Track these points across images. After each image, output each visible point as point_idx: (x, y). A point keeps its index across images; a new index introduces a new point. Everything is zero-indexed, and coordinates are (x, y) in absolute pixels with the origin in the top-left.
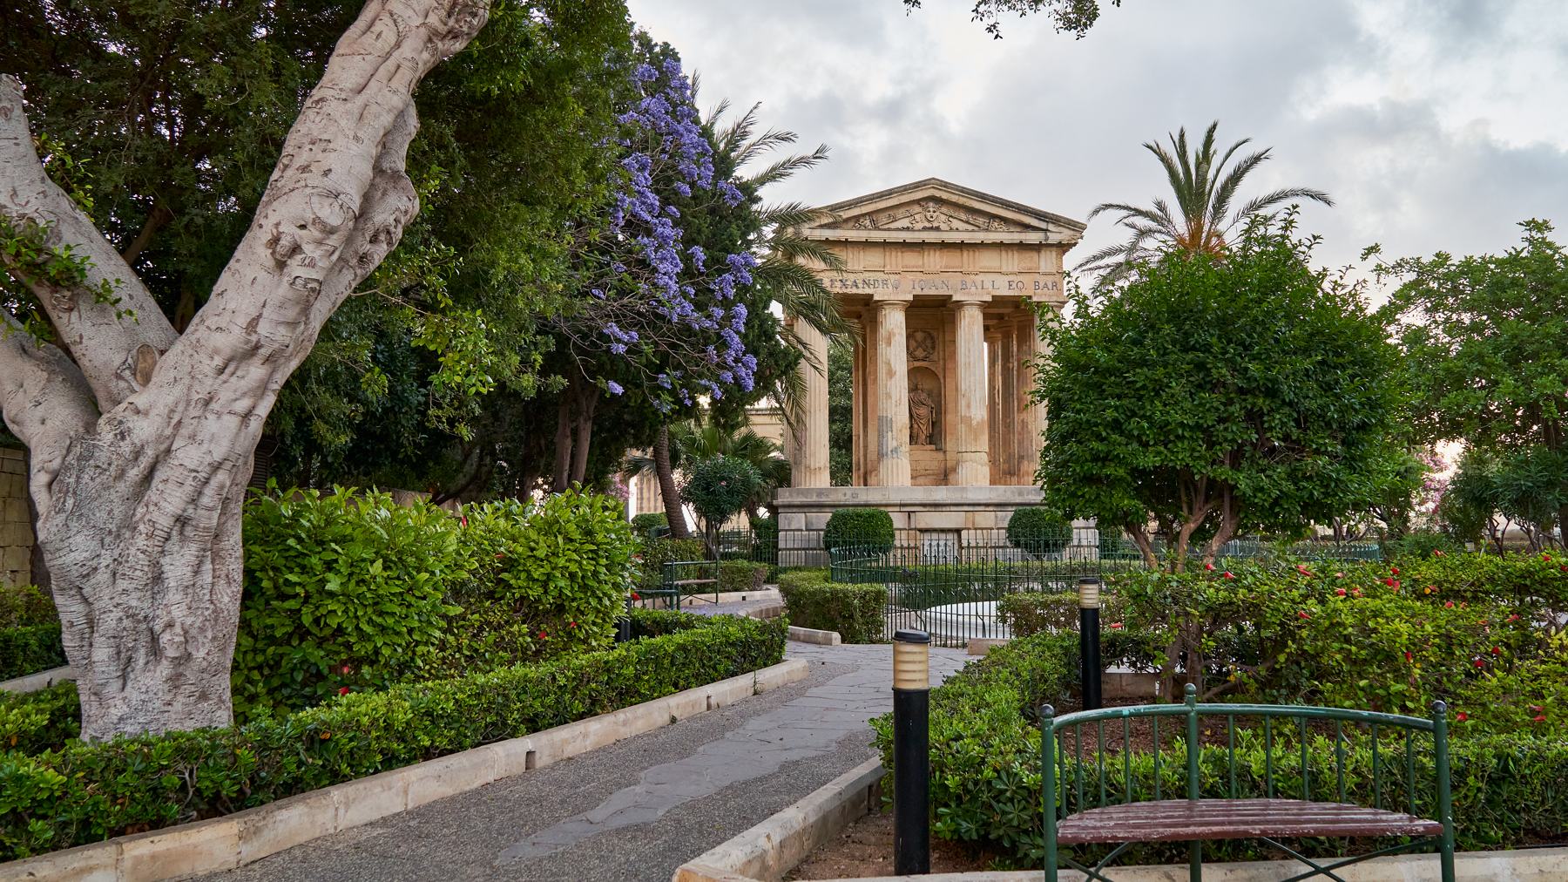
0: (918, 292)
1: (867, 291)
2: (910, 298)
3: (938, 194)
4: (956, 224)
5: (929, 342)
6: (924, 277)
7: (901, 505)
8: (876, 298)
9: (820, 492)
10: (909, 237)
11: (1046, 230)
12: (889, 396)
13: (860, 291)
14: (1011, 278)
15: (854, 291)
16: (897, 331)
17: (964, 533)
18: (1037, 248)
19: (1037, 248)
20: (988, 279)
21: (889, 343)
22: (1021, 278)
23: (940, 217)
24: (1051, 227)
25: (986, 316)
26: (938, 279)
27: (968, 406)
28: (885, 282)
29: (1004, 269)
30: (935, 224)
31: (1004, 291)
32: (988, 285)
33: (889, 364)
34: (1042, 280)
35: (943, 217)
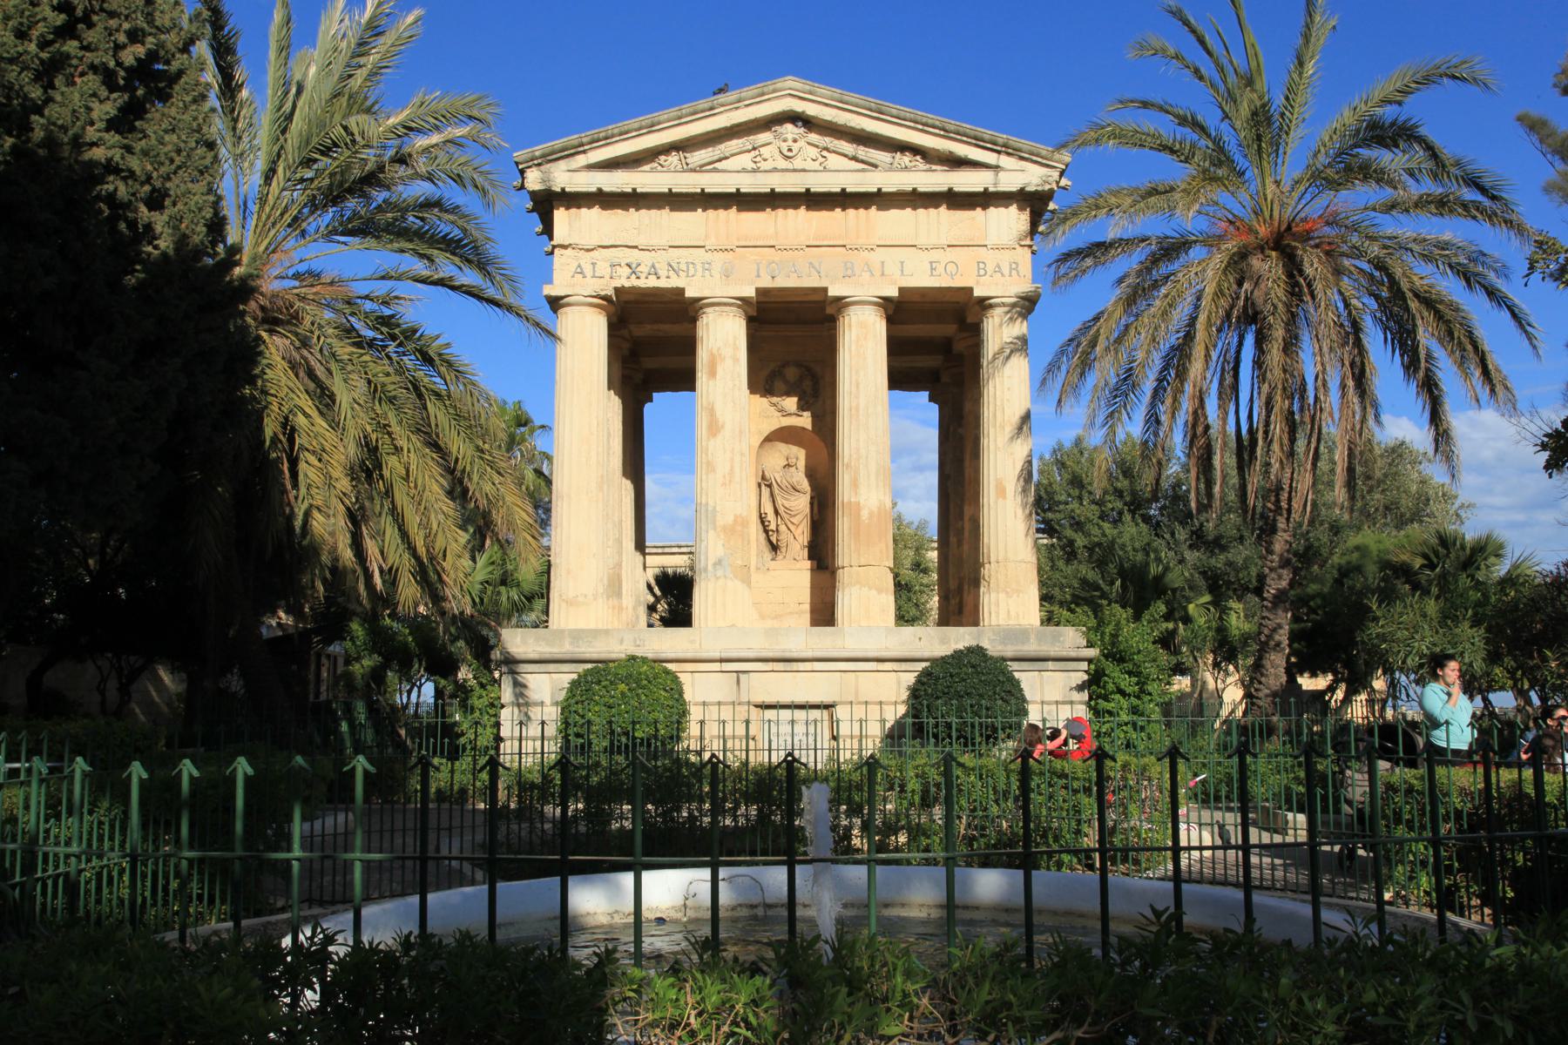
0: (766, 283)
3: (799, 106)
4: (834, 161)
5: (807, 384)
7: (722, 661)
8: (689, 294)
9: (577, 635)
10: (749, 184)
11: (996, 168)
12: (711, 467)
13: (663, 283)
14: (935, 255)
15: (652, 283)
17: (841, 712)
18: (985, 199)
19: (985, 199)
20: (891, 257)
21: (713, 373)
22: (952, 254)
23: (806, 146)
24: (1005, 161)
25: (891, 321)
27: (855, 484)
28: (707, 266)
29: (922, 241)
30: (798, 163)
31: (921, 278)
32: (892, 269)
33: (712, 412)
34: (991, 258)
35: (813, 152)
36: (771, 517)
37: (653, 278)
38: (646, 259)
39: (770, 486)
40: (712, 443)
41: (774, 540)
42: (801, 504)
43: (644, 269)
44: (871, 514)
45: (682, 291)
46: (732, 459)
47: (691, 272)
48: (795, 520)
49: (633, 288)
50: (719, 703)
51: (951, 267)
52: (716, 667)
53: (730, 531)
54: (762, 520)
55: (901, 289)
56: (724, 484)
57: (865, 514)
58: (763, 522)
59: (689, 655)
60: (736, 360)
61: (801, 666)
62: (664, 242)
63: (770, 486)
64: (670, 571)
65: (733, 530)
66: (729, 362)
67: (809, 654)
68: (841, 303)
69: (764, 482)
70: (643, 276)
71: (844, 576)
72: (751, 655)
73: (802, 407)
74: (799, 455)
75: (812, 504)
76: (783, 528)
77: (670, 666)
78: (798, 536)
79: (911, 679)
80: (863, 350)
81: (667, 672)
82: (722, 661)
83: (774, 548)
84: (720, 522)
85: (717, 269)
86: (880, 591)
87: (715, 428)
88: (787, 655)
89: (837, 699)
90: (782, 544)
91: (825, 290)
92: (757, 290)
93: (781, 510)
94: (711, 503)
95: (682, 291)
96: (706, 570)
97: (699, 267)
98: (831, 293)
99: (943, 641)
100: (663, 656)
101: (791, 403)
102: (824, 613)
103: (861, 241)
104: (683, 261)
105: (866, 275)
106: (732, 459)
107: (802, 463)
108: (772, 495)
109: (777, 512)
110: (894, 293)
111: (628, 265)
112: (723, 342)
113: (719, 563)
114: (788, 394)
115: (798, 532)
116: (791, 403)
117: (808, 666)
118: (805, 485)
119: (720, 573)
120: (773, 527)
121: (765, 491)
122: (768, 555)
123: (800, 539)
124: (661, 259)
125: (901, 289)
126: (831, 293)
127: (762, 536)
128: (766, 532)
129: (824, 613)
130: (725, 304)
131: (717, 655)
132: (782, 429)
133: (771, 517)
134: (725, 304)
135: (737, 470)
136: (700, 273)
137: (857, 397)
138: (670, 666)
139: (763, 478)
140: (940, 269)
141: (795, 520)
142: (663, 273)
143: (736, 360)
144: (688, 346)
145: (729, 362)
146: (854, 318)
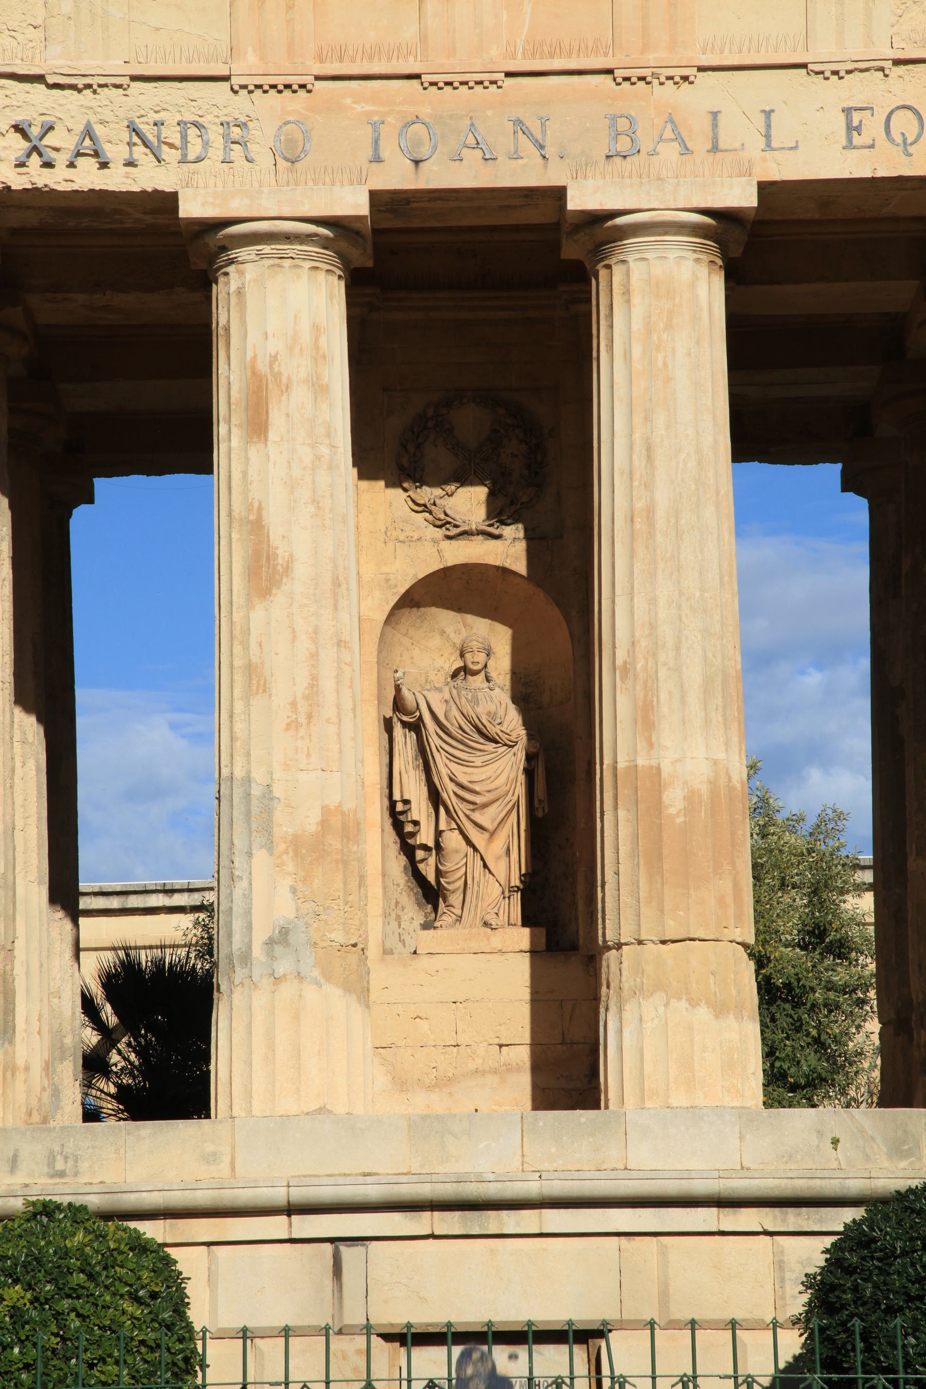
0: (397, 177)
1: (148, 177)
2: (354, 203)
6: (428, 103)
7: (291, 1210)
8: (191, 208)
12: (257, 680)
13: (116, 180)
14: (858, 89)
15: (87, 178)
16: (296, 368)
21: (258, 427)
25: (737, 275)
26: (491, 110)
27: (646, 720)
28: (236, 134)
29: (822, 50)
31: (821, 155)
32: (741, 132)
33: (257, 527)
36: (420, 809)
37: (87, 165)
38: (70, 110)
39: (416, 727)
40: (258, 615)
41: (428, 871)
42: (500, 775)
43: (62, 140)
44: (691, 799)
45: (170, 200)
46: (314, 655)
47: (195, 149)
49: (35, 192)
50: (287, 1332)
51: (904, 123)
52: (276, 1226)
53: (309, 851)
54: (397, 817)
55: (764, 188)
56: (292, 726)
57: (674, 799)
58: (398, 826)
59: (202, 1198)
60: (320, 389)
61: (511, 1221)
62: (115, 66)
63: (416, 727)
64: (144, 958)
65: (319, 849)
66: (300, 396)
67: (532, 1188)
68: (601, 232)
70: (61, 160)
71: (621, 969)
72: (373, 1192)
73: (501, 511)
74: (495, 641)
75: (529, 773)
76: (452, 840)
77: (151, 1230)
78: (493, 858)
79: (811, 1255)
80: (662, 355)
81: (142, 1247)
82: (291, 1210)
83: (431, 894)
84: (284, 826)
85: (262, 141)
86: (720, 1010)
87: (266, 574)
88: (472, 1190)
89: (608, 1313)
90: (452, 883)
91: (559, 193)
92: (375, 196)
93: (448, 791)
94: (259, 776)
95: (172, 198)
96: (246, 958)
97: (215, 135)
98: (576, 202)
99: (901, 1147)
100: (130, 1201)
101: (469, 502)
102: (568, 1073)
103: (652, 58)
104: (170, 118)
105: (669, 152)
106: (314, 655)
107: (501, 664)
108: (422, 751)
109: (435, 798)
110: (743, 197)
111: (17, 128)
112: (285, 334)
113: (281, 938)
114: (463, 479)
115: (494, 850)
116: (469, 502)
117: (527, 1220)
118: (512, 722)
119: (283, 966)
120: (426, 836)
121: (405, 742)
122: (413, 913)
123: (499, 868)
124: (110, 113)
125: (764, 188)
126: (576, 202)
127: (397, 863)
128: (408, 850)
129: (568, 1073)
130: (288, 238)
131: (278, 1195)
132: (446, 573)
133: (420, 809)
134: (288, 238)
135: (328, 684)
136: (216, 152)
137: (649, 486)
138: (151, 1230)
139: (398, 704)
140: (873, 127)
142: (115, 152)
143: (320, 389)
144: (190, 350)
145: (300, 396)
146: (637, 269)
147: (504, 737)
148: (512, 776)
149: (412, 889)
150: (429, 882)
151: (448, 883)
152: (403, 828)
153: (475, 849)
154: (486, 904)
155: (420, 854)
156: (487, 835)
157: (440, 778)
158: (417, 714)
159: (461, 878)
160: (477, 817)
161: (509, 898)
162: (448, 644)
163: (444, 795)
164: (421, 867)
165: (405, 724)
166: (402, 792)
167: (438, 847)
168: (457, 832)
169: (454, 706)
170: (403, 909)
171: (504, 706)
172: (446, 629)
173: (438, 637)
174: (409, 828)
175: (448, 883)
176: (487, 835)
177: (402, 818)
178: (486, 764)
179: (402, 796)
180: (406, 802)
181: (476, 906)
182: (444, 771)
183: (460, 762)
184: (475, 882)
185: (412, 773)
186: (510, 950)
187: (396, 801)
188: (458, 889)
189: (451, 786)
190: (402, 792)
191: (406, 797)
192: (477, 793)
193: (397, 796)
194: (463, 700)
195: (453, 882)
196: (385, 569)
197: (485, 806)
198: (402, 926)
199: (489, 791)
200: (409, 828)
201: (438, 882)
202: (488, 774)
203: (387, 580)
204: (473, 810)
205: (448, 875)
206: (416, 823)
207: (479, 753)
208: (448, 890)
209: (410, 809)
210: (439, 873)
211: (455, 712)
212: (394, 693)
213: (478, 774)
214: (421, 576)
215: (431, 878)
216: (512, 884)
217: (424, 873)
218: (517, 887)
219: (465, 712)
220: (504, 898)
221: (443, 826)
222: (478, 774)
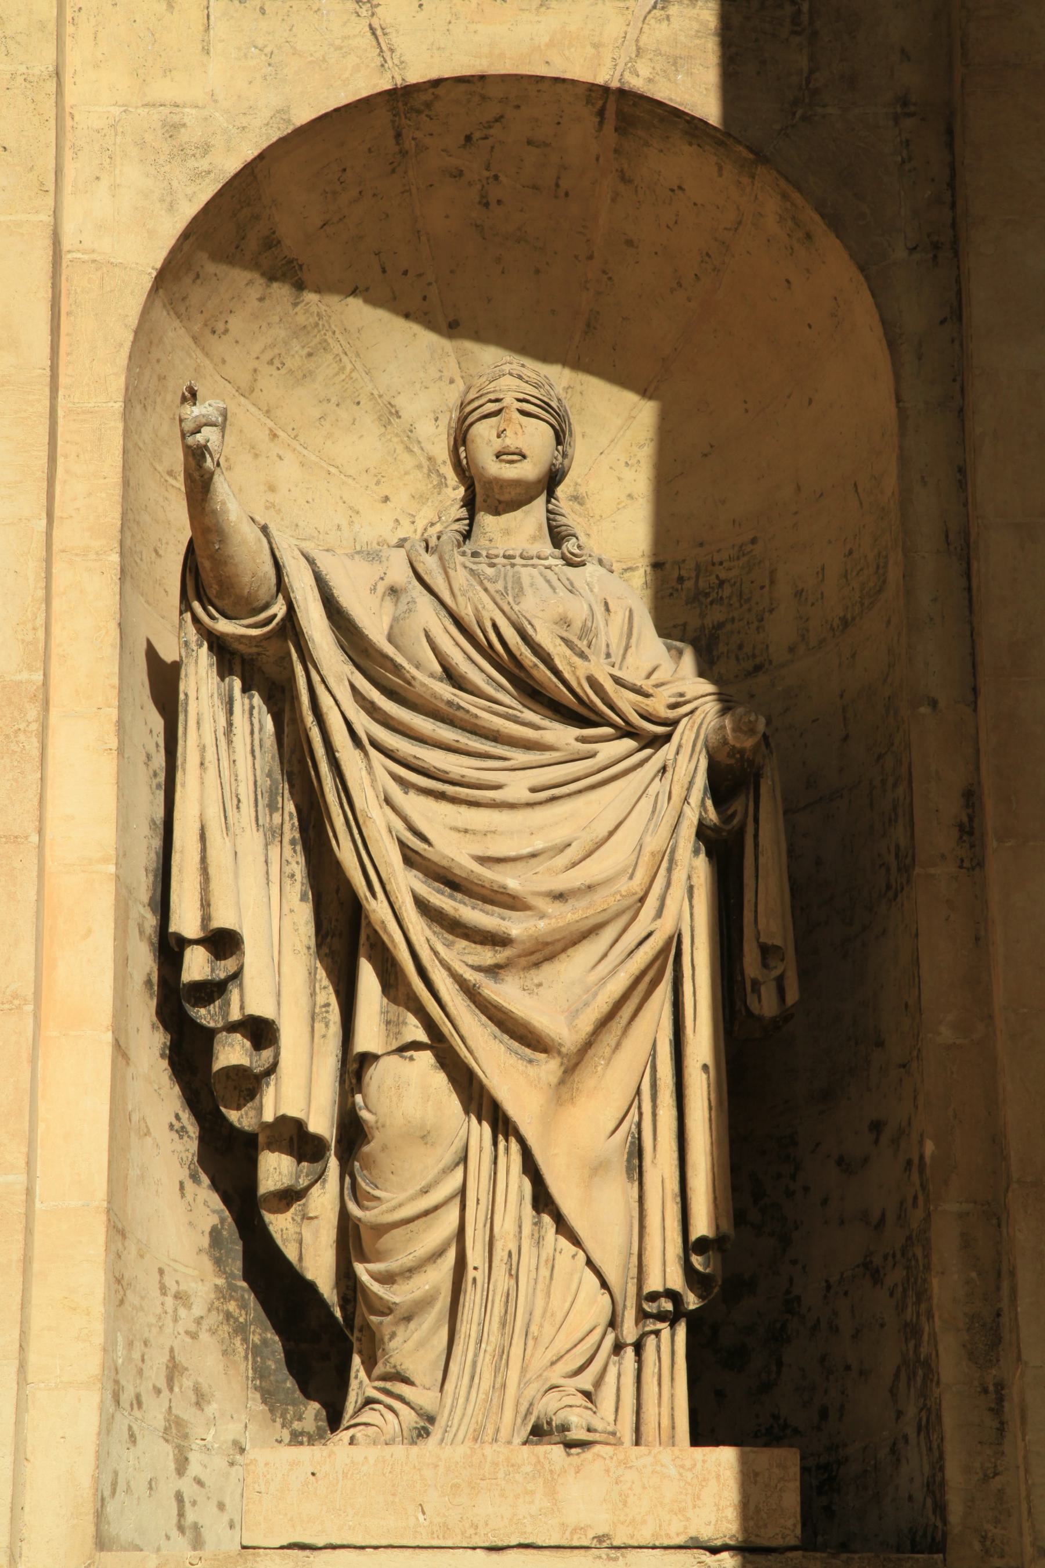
36: (279, 974)
39: (266, 668)
41: (309, 1243)
48: (554, 1001)
54: (187, 1012)
58: (188, 1052)
69: (239, 630)
75: (723, 849)
76: (410, 1093)
83: (317, 1345)
90: (408, 1279)
93: (396, 899)
108: (302, 777)
109: (344, 934)
115: (577, 1132)
120: (301, 1088)
121: (226, 734)
123: (601, 1211)
127: (184, 1218)
128: (227, 1158)
133: (279, 974)
139: (205, 577)
141: (554, 1001)
147: (625, 700)
148: (655, 842)
149: (241, 1330)
150: (311, 1287)
151: (387, 1279)
152: (209, 1054)
153: (502, 1124)
154: (540, 1359)
155: (275, 1169)
156: (549, 1068)
157: (363, 845)
158: (279, 609)
159: (438, 1254)
160: (509, 993)
161: (638, 1347)
162: (409, 461)
163: (378, 909)
164: (280, 1225)
165: (227, 656)
166: (205, 904)
167: (353, 1132)
168: (426, 1058)
169: (424, 600)
170: (200, 1399)
171: (619, 618)
172: (400, 402)
173: (369, 423)
174: (233, 1053)
175: (387, 1279)
176: (549, 1068)
177: (205, 1016)
178: (547, 795)
179: (206, 919)
180: (223, 943)
181: (503, 1354)
182: (379, 822)
183: (443, 788)
184: (500, 1254)
185: (251, 840)
186: (645, 1536)
187: (183, 943)
188: (424, 1303)
189: (405, 882)
190: (205, 904)
191: (223, 919)
192: (510, 902)
193: (186, 922)
194: (460, 577)
195: (410, 1272)
196: (164, 90)
197: (545, 952)
198: (194, 1468)
199: (560, 897)
200: (233, 1053)
201: (346, 1276)
202: (559, 835)
203: (172, 129)
204: (493, 971)
205: (387, 1241)
206: (261, 1032)
207: (521, 757)
208: (387, 1310)
209: (236, 975)
210: (351, 1240)
211: (427, 615)
212: (188, 534)
213: (510, 832)
214: (303, 116)
215: (319, 1268)
216: (654, 1284)
217: (291, 1253)
218: (672, 1295)
219: (467, 613)
220: (618, 1348)
221: (369, 1036)
222: (510, 832)
